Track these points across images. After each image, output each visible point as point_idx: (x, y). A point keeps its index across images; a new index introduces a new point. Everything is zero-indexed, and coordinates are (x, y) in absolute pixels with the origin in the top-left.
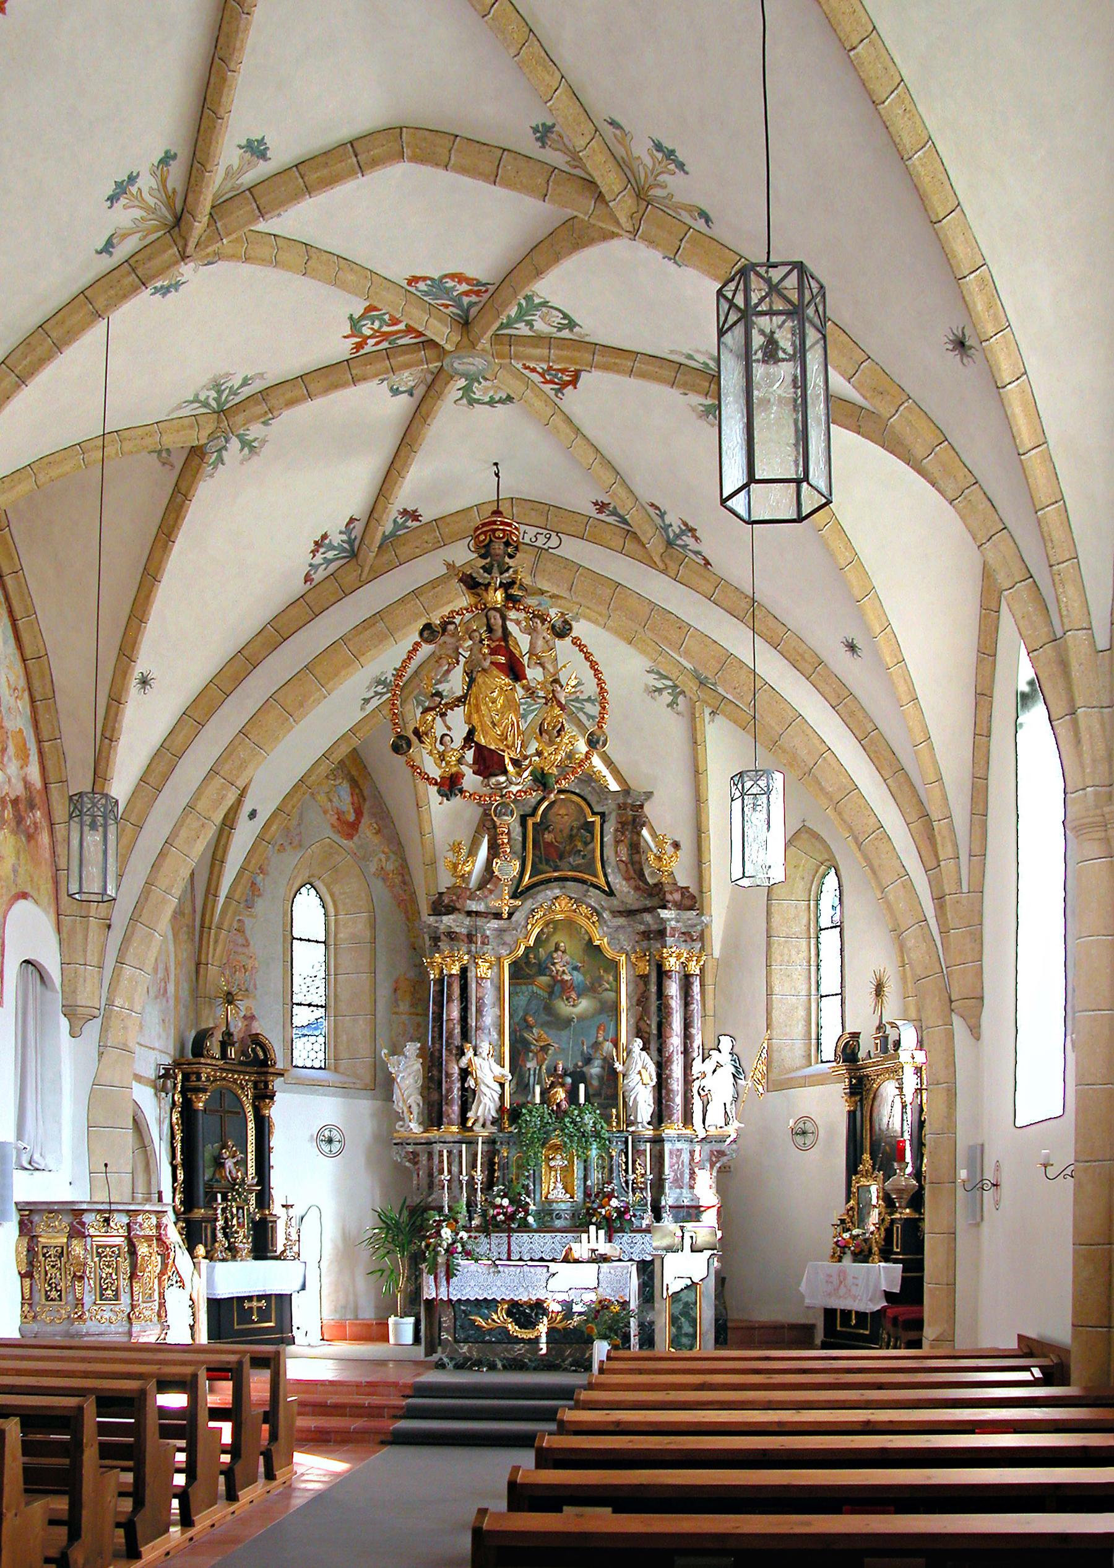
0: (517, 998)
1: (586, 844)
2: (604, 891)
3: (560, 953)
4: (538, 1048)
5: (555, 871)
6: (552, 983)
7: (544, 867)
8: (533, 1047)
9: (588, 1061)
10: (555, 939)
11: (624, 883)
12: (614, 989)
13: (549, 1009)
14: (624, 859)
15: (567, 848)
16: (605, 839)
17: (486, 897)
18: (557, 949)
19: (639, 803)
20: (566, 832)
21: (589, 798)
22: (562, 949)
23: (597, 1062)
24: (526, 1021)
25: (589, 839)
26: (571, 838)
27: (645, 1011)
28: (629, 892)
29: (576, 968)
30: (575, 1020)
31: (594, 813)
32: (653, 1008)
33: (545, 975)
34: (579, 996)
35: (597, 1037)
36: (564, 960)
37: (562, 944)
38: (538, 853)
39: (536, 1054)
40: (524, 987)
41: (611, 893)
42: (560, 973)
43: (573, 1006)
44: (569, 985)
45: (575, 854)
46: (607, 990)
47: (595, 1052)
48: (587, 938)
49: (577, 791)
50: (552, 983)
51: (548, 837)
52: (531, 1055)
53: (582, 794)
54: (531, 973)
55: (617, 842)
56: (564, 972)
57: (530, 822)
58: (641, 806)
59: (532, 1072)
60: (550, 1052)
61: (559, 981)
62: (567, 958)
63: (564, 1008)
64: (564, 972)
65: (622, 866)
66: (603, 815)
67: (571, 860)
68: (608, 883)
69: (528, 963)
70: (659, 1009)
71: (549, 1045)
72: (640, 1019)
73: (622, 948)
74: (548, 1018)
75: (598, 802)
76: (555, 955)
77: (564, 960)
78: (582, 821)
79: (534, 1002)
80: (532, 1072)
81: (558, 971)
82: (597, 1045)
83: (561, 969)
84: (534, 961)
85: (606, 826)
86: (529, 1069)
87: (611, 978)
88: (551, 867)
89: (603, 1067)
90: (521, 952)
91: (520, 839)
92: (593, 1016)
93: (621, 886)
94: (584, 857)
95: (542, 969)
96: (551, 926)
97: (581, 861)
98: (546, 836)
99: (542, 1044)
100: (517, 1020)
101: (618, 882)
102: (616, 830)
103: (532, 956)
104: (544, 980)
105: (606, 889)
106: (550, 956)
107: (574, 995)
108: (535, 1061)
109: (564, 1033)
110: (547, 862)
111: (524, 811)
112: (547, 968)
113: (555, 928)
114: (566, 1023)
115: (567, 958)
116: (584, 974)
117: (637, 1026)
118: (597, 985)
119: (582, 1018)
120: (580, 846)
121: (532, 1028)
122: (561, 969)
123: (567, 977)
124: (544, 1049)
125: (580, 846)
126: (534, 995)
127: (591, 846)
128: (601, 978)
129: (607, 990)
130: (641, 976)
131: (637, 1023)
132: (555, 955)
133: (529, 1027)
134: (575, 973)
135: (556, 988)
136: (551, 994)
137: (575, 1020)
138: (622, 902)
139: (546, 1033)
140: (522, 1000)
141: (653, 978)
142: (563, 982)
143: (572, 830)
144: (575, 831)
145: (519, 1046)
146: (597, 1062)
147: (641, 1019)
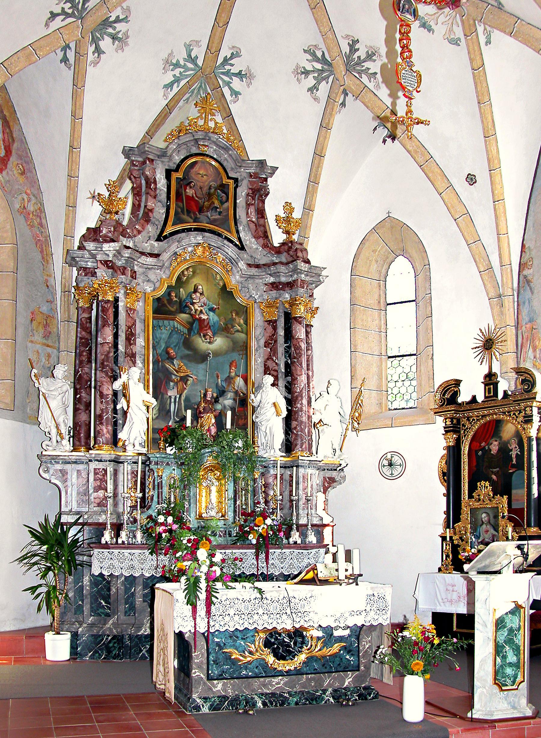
0: (159, 331)
1: (222, 203)
2: (236, 245)
3: (198, 294)
4: (179, 378)
5: (194, 222)
6: (191, 320)
7: (185, 217)
8: (173, 377)
9: (222, 393)
10: (196, 281)
11: (254, 239)
12: (245, 331)
13: (187, 344)
14: (254, 220)
15: (206, 203)
16: (238, 201)
17: (135, 236)
18: (196, 291)
19: (264, 176)
20: (205, 189)
21: (225, 164)
22: (200, 291)
23: (230, 395)
24: (168, 353)
25: (224, 199)
26: (210, 195)
27: (274, 351)
28: (257, 249)
29: (212, 310)
30: (211, 356)
31: (229, 178)
32: (281, 350)
33: (185, 313)
34: (214, 334)
35: (230, 372)
36: (202, 300)
37: (200, 287)
38: (180, 204)
39: (176, 383)
40: (166, 322)
41: (242, 248)
42: (198, 313)
43: (210, 343)
44: (206, 323)
45: (212, 210)
46: (238, 331)
47: (228, 386)
48: (221, 284)
49: (215, 156)
50: (191, 320)
51: (190, 192)
52: (172, 384)
53: (219, 159)
54: (173, 309)
55: (248, 205)
56: (201, 312)
57: (174, 176)
58: (266, 180)
59: (173, 400)
60: (189, 382)
61: (197, 319)
62: (204, 299)
63: (201, 344)
64: (201, 312)
65: (252, 226)
66: (236, 180)
67: (209, 214)
68: (240, 239)
69: (170, 301)
70: (287, 351)
71: (188, 376)
72: (268, 359)
73: (251, 296)
74: (187, 352)
75: (232, 169)
76: (194, 296)
77: (202, 300)
78: (219, 183)
79: (175, 336)
80: (173, 400)
81: (196, 310)
82: (229, 380)
83: (199, 309)
84: (175, 299)
85: (238, 190)
86: (170, 397)
87: (242, 321)
88: (191, 218)
89: (234, 400)
90: (164, 290)
91: (166, 190)
92: (226, 352)
93: (251, 242)
94: (220, 213)
95: (183, 307)
96: (191, 270)
97: (218, 217)
98: (187, 191)
99: (182, 375)
100: (159, 351)
101: (247, 237)
102: (248, 195)
103: (173, 294)
104: (184, 316)
105: (238, 243)
106: (190, 296)
107: (210, 333)
108: (175, 390)
109: (202, 366)
110: (189, 212)
111: (169, 166)
112: (186, 306)
113: (194, 272)
114: (203, 358)
115: (204, 299)
116: (219, 316)
117: (265, 365)
118: (230, 326)
119: (216, 354)
120: (217, 203)
121: (173, 359)
122: (199, 309)
123: (204, 317)
124: (184, 379)
125: (217, 203)
126: (174, 330)
127: (226, 205)
128: (233, 320)
129: (238, 331)
130: (269, 322)
131: (265, 362)
132: (194, 296)
133: (171, 359)
134: (211, 314)
135: (194, 325)
136: (190, 330)
137: (211, 356)
138: (252, 256)
139: (185, 365)
140: (164, 334)
141: (281, 324)
142: (201, 321)
143: (210, 188)
144: (212, 190)
145: (160, 375)
146: (230, 395)
147: (269, 358)
